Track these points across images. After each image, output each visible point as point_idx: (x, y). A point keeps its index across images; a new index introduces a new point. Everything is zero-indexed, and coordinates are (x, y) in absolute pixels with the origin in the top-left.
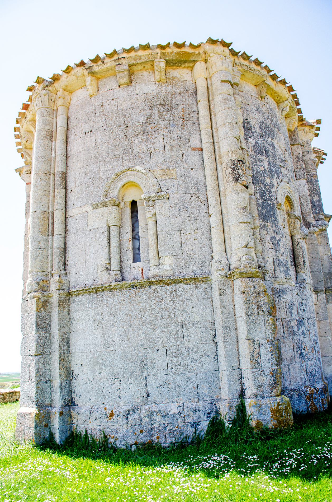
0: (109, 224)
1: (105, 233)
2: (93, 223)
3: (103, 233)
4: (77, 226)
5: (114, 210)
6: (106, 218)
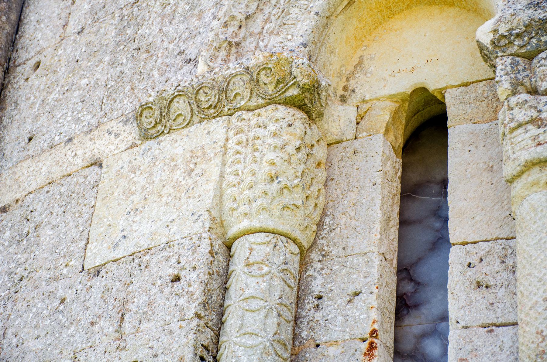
0: (227, 219)
1: (193, 276)
2: (122, 223)
3: (177, 279)
4: (22, 257)
5: (272, 127)
6: (212, 186)
